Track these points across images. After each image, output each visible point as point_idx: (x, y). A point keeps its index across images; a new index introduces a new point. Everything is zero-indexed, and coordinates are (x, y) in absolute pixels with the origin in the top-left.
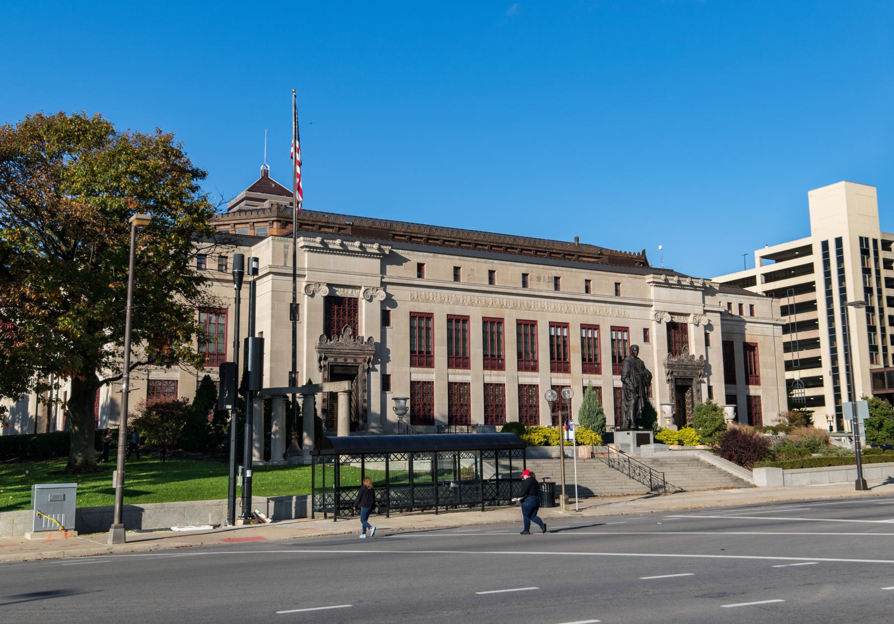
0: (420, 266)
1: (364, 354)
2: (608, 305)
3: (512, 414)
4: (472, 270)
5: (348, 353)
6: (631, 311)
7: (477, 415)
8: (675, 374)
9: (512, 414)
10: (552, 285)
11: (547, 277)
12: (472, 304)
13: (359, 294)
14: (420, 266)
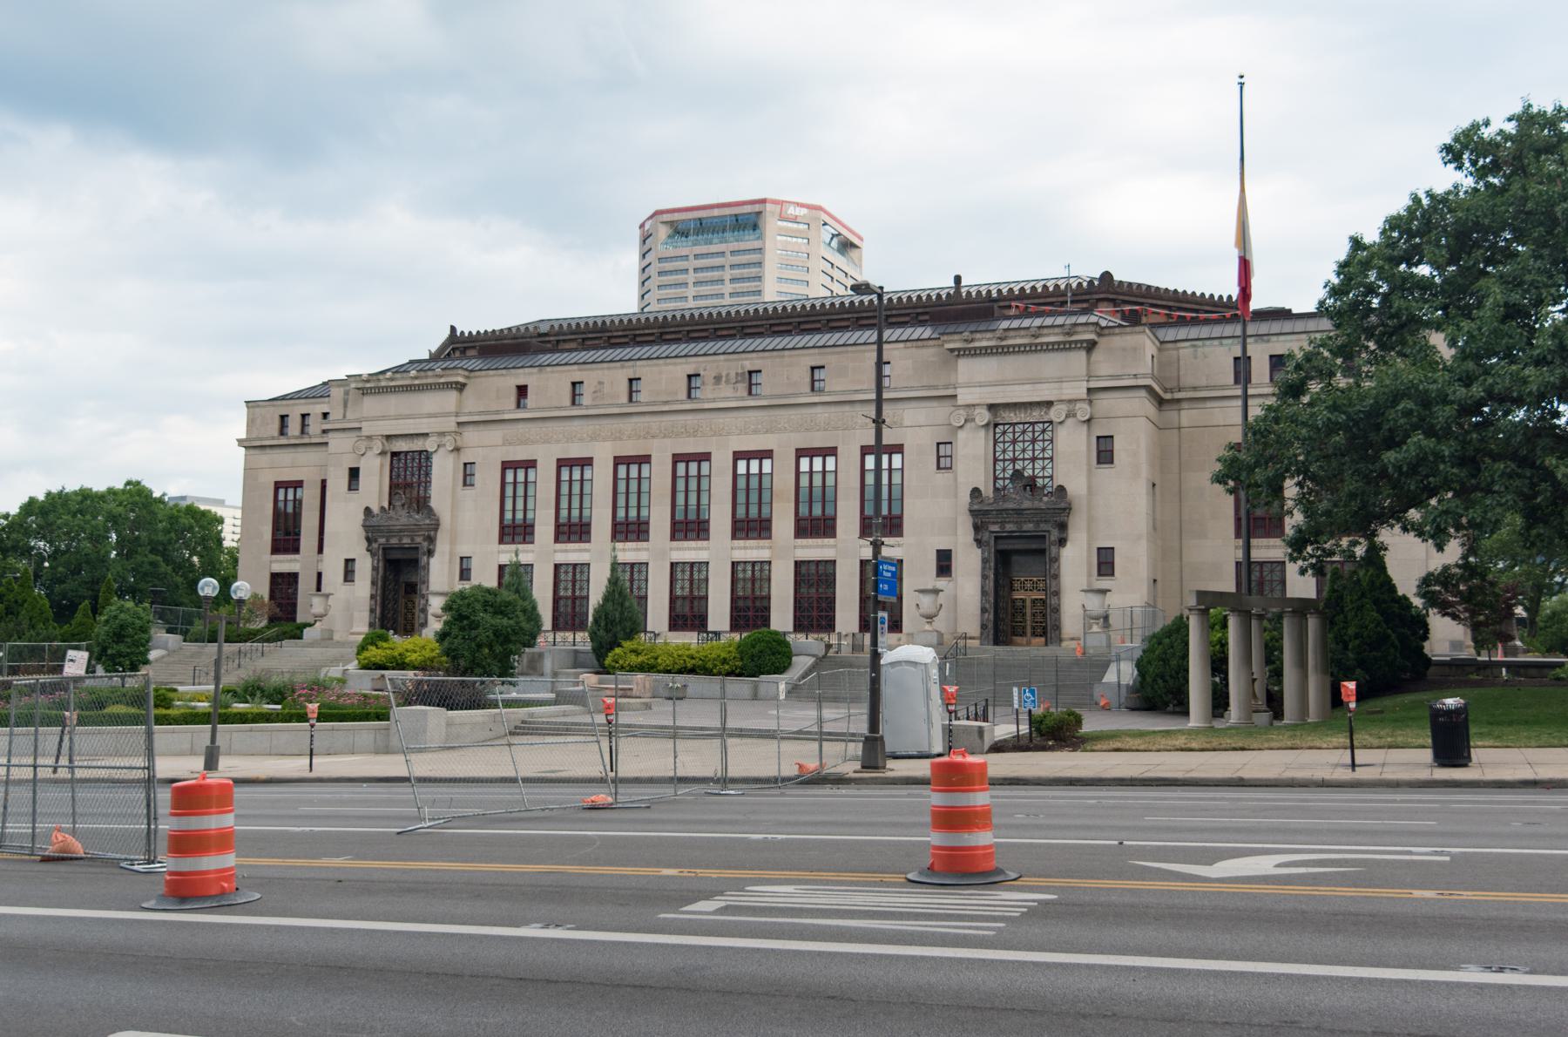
0: (522, 391)
4: (600, 383)
7: (719, 613)
8: (995, 528)
10: (742, 389)
11: (733, 375)
12: (594, 438)
13: (430, 445)
14: (522, 391)
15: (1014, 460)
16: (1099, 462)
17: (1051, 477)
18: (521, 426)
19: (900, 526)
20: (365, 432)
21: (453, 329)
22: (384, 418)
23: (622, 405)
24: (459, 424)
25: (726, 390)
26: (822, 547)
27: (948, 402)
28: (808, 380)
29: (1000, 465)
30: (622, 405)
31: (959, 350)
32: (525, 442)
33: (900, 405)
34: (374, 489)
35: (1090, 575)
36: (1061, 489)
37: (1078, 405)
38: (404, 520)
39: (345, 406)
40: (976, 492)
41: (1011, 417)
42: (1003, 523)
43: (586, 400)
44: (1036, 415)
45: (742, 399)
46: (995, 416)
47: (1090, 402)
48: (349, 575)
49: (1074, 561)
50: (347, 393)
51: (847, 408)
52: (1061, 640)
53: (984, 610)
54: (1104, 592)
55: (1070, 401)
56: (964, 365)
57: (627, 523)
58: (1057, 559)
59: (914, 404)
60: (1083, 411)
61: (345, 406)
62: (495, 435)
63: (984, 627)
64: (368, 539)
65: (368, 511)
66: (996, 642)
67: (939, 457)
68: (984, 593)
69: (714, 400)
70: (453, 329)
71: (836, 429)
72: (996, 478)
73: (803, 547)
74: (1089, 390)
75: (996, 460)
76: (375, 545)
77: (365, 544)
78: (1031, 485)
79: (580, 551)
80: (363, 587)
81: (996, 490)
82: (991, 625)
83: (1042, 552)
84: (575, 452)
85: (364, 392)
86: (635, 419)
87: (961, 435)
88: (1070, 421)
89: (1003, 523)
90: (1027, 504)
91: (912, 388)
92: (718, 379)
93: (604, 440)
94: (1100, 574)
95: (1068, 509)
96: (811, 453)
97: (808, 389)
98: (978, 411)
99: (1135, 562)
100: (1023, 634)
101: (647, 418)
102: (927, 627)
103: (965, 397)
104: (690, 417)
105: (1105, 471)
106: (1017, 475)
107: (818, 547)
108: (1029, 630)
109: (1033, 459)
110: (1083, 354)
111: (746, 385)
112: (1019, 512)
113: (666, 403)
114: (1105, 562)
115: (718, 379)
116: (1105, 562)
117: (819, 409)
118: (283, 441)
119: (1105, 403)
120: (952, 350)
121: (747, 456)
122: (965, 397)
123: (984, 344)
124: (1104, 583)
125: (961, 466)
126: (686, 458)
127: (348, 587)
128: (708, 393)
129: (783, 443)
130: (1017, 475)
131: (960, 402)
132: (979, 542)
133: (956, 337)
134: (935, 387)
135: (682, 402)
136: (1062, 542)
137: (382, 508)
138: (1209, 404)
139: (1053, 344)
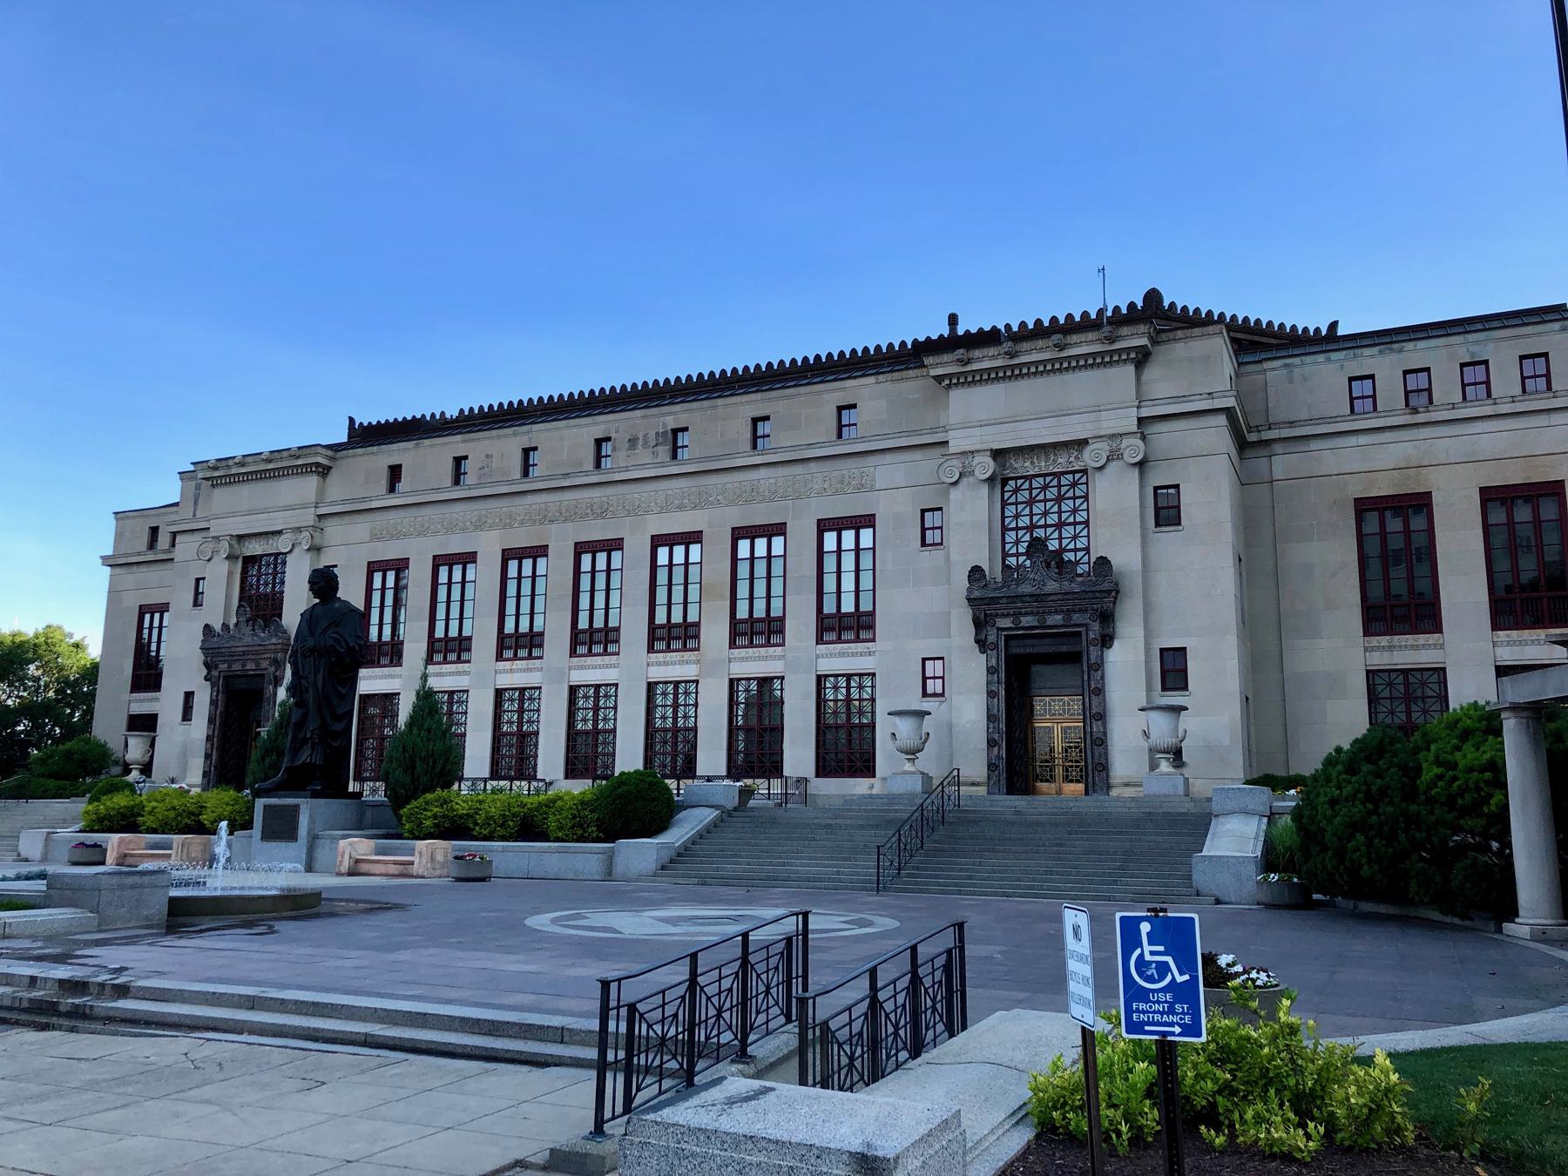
0: (395, 472)
1: (267, 651)
2: (813, 465)
3: (629, 756)
4: (488, 456)
5: (244, 653)
6: (888, 472)
8: (1005, 623)
9: (629, 756)
10: (664, 451)
11: (652, 435)
13: (282, 545)
14: (395, 472)
15: (1032, 527)
16: (1157, 525)
17: (1087, 550)
18: (392, 515)
19: (871, 627)
20: (212, 533)
21: (351, 420)
22: (234, 514)
23: (512, 482)
24: (320, 516)
25: (643, 455)
26: (766, 658)
27: (938, 451)
28: (748, 435)
29: (1011, 537)
30: (512, 482)
31: (950, 376)
32: (396, 535)
33: (871, 460)
34: (220, 605)
35: (1149, 689)
36: (1103, 562)
37: (1125, 442)
38: (248, 640)
39: (196, 503)
40: (976, 573)
41: (1026, 466)
42: (1017, 616)
43: (469, 479)
44: (1062, 462)
45: (662, 465)
46: (1004, 467)
47: (1144, 438)
48: (187, 715)
49: (1126, 666)
50: (198, 487)
51: (798, 470)
52: (1109, 787)
53: (991, 743)
54: (1178, 710)
55: (1112, 437)
56: (957, 396)
57: (517, 634)
58: (1099, 665)
59: (888, 458)
60: (1133, 449)
61: (196, 503)
62: (360, 528)
63: (991, 767)
64: (206, 664)
65: (208, 629)
66: (1011, 791)
67: (923, 530)
68: (991, 717)
69: (627, 469)
70: (351, 420)
71: (784, 497)
72: (1005, 555)
73: (742, 659)
74: (1140, 420)
75: (1005, 529)
76: (215, 673)
77: (205, 672)
78: (1058, 563)
79: (458, 673)
80: (199, 727)
81: (1006, 567)
82: (1002, 765)
83: (1074, 658)
84: (456, 546)
85: (215, 482)
86: (530, 499)
87: (955, 494)
88: (1113, 465)
89: (1017, 616)
90: (1052, 586)
91: (886, 437)
92: (633, 442)
93: (491, 528)
94: (1164, 688)
95: (1115, 592)
96: (751, 533)
97: (748, 446)
98: (978, 459)
99: (1217, 671)
100: (1051, 779)
101: (544, 497)
102: (908, 767)
103: (958, 442)
104: (596, 493)
105: (1167, 538)
106: (1037, 546)
107: (760, 658)
108: (1059, 771)
109: (1060, 525)
110: (1131, 368)
111: (668, 447)
112: (1039, 598)
113: (566, 475)
114: (1173, 669)
115: (633, 442)
116: (1173, 669)
117: (763, 472)
118: (151, 557)
119: (1166, 437)
120: (939, 379)
121: (670, 540)
122: (958, 442)
123: (986, 365)
124: (1175, 699)
125: (953, 539)
126: (592, 547)
127: (183, 728)
128: (618, 461)
129: (716, 521)
130: (1037, 546)
131: (952, 450)
132: (982, 644)
133: (946, 358)
134: (918, 433)
135: (586, 473)
136: (1107, 640)
137: (225, 626)
138: (1314, 445)
139: (1086, 356)
